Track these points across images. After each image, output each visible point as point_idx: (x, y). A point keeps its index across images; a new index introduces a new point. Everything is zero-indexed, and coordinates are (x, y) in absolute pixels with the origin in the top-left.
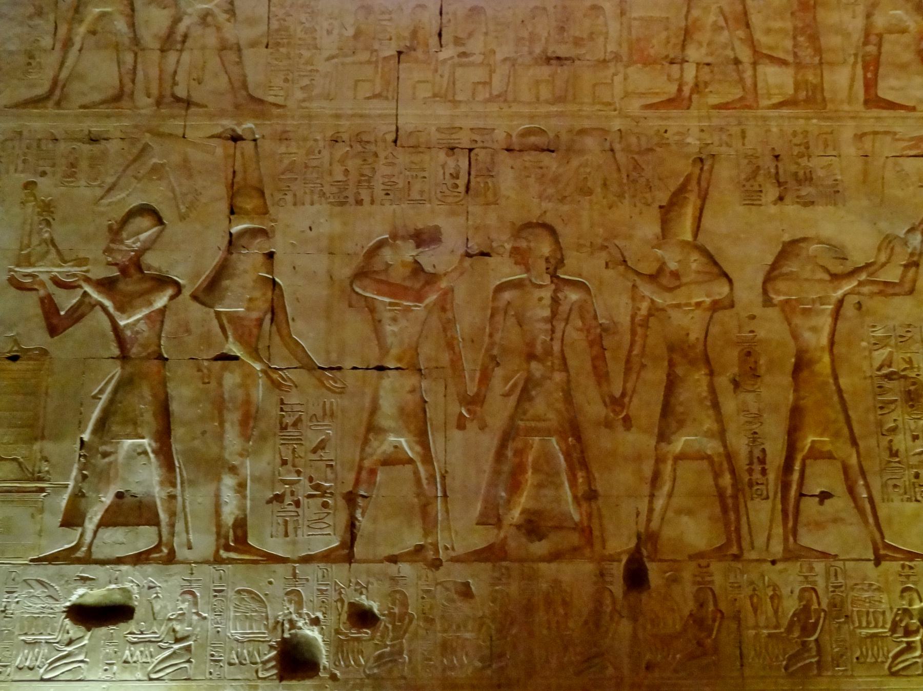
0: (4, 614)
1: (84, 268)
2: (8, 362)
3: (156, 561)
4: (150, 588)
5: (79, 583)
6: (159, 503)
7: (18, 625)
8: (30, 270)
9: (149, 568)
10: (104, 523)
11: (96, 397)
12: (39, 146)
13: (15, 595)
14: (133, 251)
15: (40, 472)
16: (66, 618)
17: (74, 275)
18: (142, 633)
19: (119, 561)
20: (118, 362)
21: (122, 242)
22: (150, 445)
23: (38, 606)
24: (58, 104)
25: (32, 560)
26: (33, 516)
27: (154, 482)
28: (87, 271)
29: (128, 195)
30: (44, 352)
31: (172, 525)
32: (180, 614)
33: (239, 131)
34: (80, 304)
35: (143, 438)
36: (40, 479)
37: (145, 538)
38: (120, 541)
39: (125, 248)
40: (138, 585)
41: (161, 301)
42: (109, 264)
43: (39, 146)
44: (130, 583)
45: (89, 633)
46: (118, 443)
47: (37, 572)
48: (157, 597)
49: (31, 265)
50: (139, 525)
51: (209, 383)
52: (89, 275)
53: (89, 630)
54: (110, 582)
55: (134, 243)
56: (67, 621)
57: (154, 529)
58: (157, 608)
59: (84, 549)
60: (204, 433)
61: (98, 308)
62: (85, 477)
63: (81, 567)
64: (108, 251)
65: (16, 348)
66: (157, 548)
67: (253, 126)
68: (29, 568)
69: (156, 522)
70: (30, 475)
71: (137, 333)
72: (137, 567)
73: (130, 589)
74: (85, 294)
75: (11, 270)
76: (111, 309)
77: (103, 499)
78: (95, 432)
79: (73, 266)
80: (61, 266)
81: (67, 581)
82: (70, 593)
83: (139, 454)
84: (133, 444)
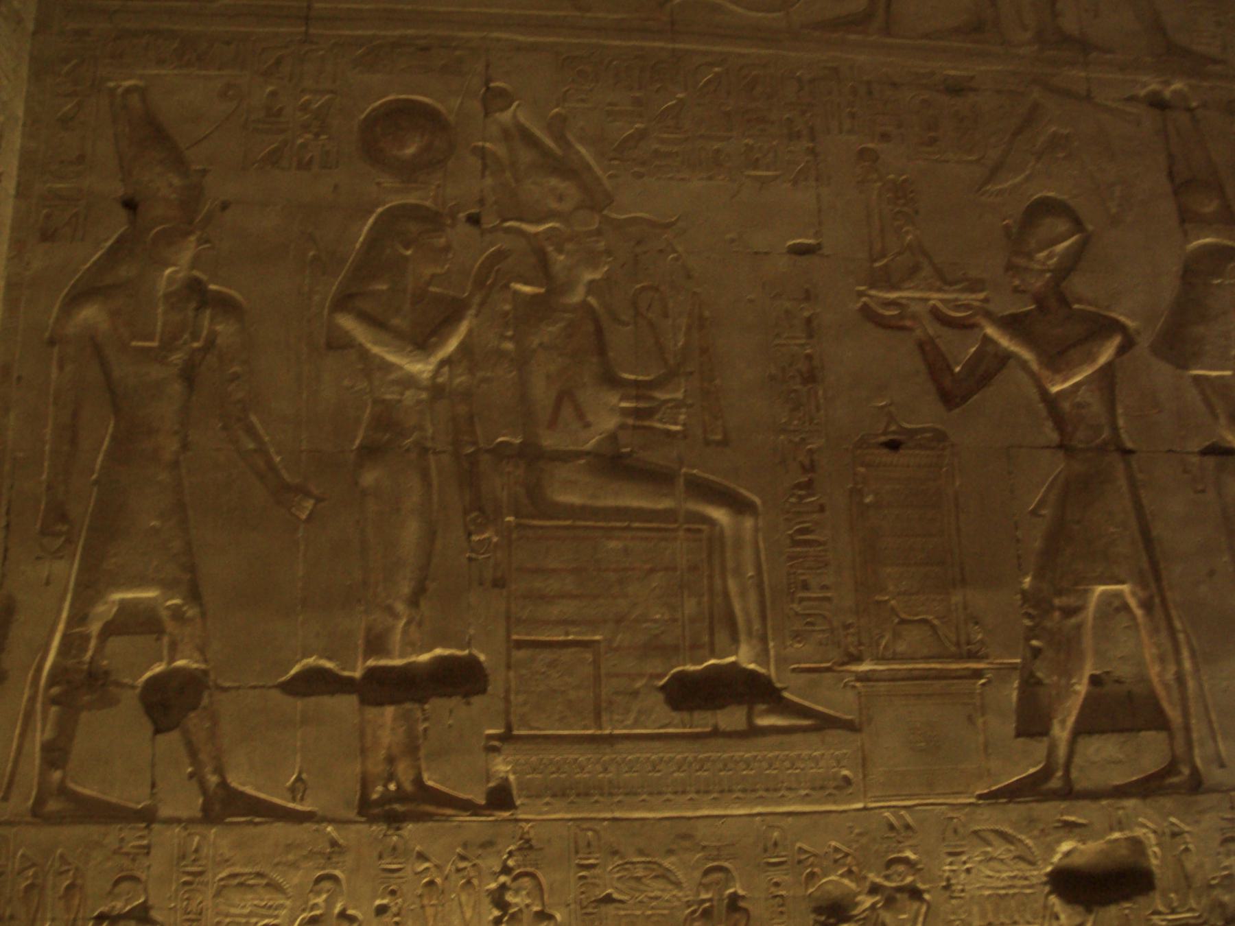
0: (948, 894)
1: (982, 296)
2: (885, 451)
3: (1174, 790)
4: (1174, 835)
5: (1062, 833)
6: (1161, 692)
7: (975, 909)
8: (893, 295)
9: (1168, 803)
10: (1083, 729)
11: (1034, 513)
12: (870, 93)
13: (964, 858)
14: (1049, 271)
15: (968, 643)
16: (1050, 893)
17: (967, 307)
18: (1173, 912)
19: (1120, 792)
20: (1061, 454)
21: (1030, 256)
22: (1134, 594)
23: (1004, 875)
24: (887, 31)
25: (980, 797)
26: (970, 719)
27: (1147, 656)
28: (986, 300)
29: (1028, 179)
30: (940, 436)
31: (1187, 729)
32: (1226, 877)
33: (1167, 94)
34: (979, 355)
35: (1122, 582)
36: (972, 656)
37: (1150, 752)
38: (1106, 759)
39: (1037, 267)
40: (1155, 832)
41: (1106, 354)
42: (1016, 290)
43: (870, 93)
44: (1144, 827)
45: (1091, 918)
46: (1086, 591)
47: (988, 819)
48: (1187, 850)
49: (894, 287)
50: (1140, 730)
51: (1203, 491)
52: (990, 307)
53: (1089, 910)
54: (1112, 830)
55: (1049, 257)
56: (1053, 899)
57: (1162, 736)
58: (1190, 865)
59: (1059, 774)
60: (1212, 573)
61: (1012, 362)
62: (1037, 652)
63: (1063, 805)
64: (1010, 268)
65: (893, 428)
66: (1171, 768)
67: (1186, 89)
68: (979, 811)
69: (1160, 722)
70: (953, 649)
71: (1079, 406)
72: (1149, 801)
73: (1143, 838)
74: (987, 340)
75: (861, 294)
76: (1035, 366)
77: (1078, 688)
78: (1039, 576)
79: (963, 290)
80: (939, 290)
81: (1042, 830)
82: (1051, 850)
83: (1117, 610)
84: (1104, 593)
